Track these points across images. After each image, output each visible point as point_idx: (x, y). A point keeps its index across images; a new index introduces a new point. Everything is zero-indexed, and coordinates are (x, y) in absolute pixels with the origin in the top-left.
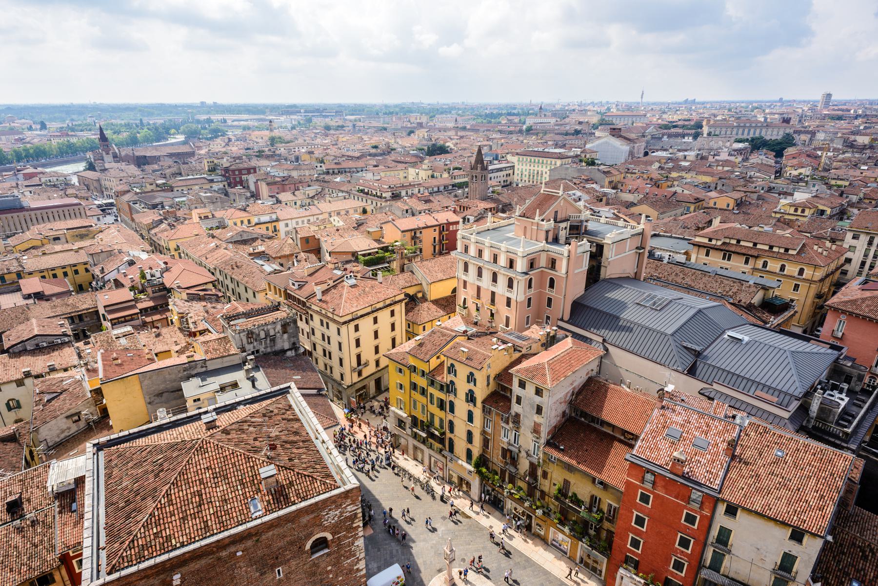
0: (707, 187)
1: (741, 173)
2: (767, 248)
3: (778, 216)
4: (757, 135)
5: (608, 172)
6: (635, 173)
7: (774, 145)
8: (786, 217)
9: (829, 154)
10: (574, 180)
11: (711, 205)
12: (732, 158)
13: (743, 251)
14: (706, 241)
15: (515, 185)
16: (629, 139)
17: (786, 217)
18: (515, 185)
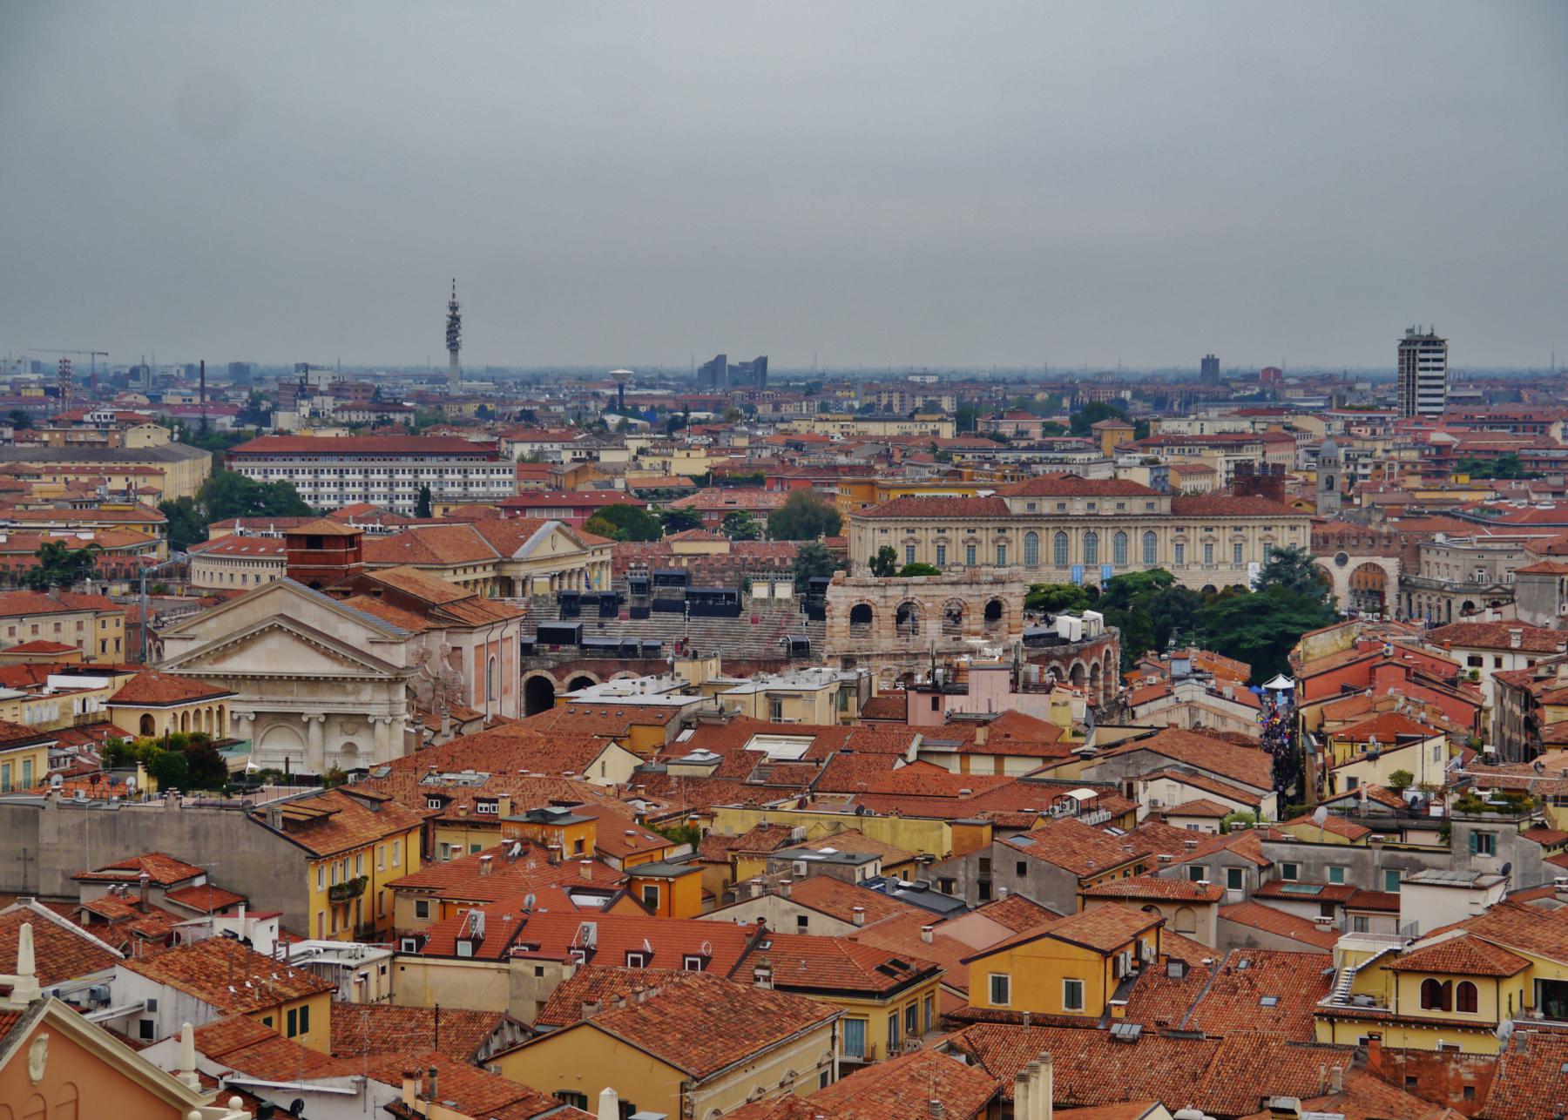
0: (936, 890)
3: (1350, 1035)
4: (1136, 565)
5: (320, 822)
6: (493, 824)
7: (1232, 621)
8: (1394, 1039)
9: (1508, 663)
10: (90, 897)
11: (981, 998)
12: (1032, 705)
16: (417, 606)
17: (1394, 1039)
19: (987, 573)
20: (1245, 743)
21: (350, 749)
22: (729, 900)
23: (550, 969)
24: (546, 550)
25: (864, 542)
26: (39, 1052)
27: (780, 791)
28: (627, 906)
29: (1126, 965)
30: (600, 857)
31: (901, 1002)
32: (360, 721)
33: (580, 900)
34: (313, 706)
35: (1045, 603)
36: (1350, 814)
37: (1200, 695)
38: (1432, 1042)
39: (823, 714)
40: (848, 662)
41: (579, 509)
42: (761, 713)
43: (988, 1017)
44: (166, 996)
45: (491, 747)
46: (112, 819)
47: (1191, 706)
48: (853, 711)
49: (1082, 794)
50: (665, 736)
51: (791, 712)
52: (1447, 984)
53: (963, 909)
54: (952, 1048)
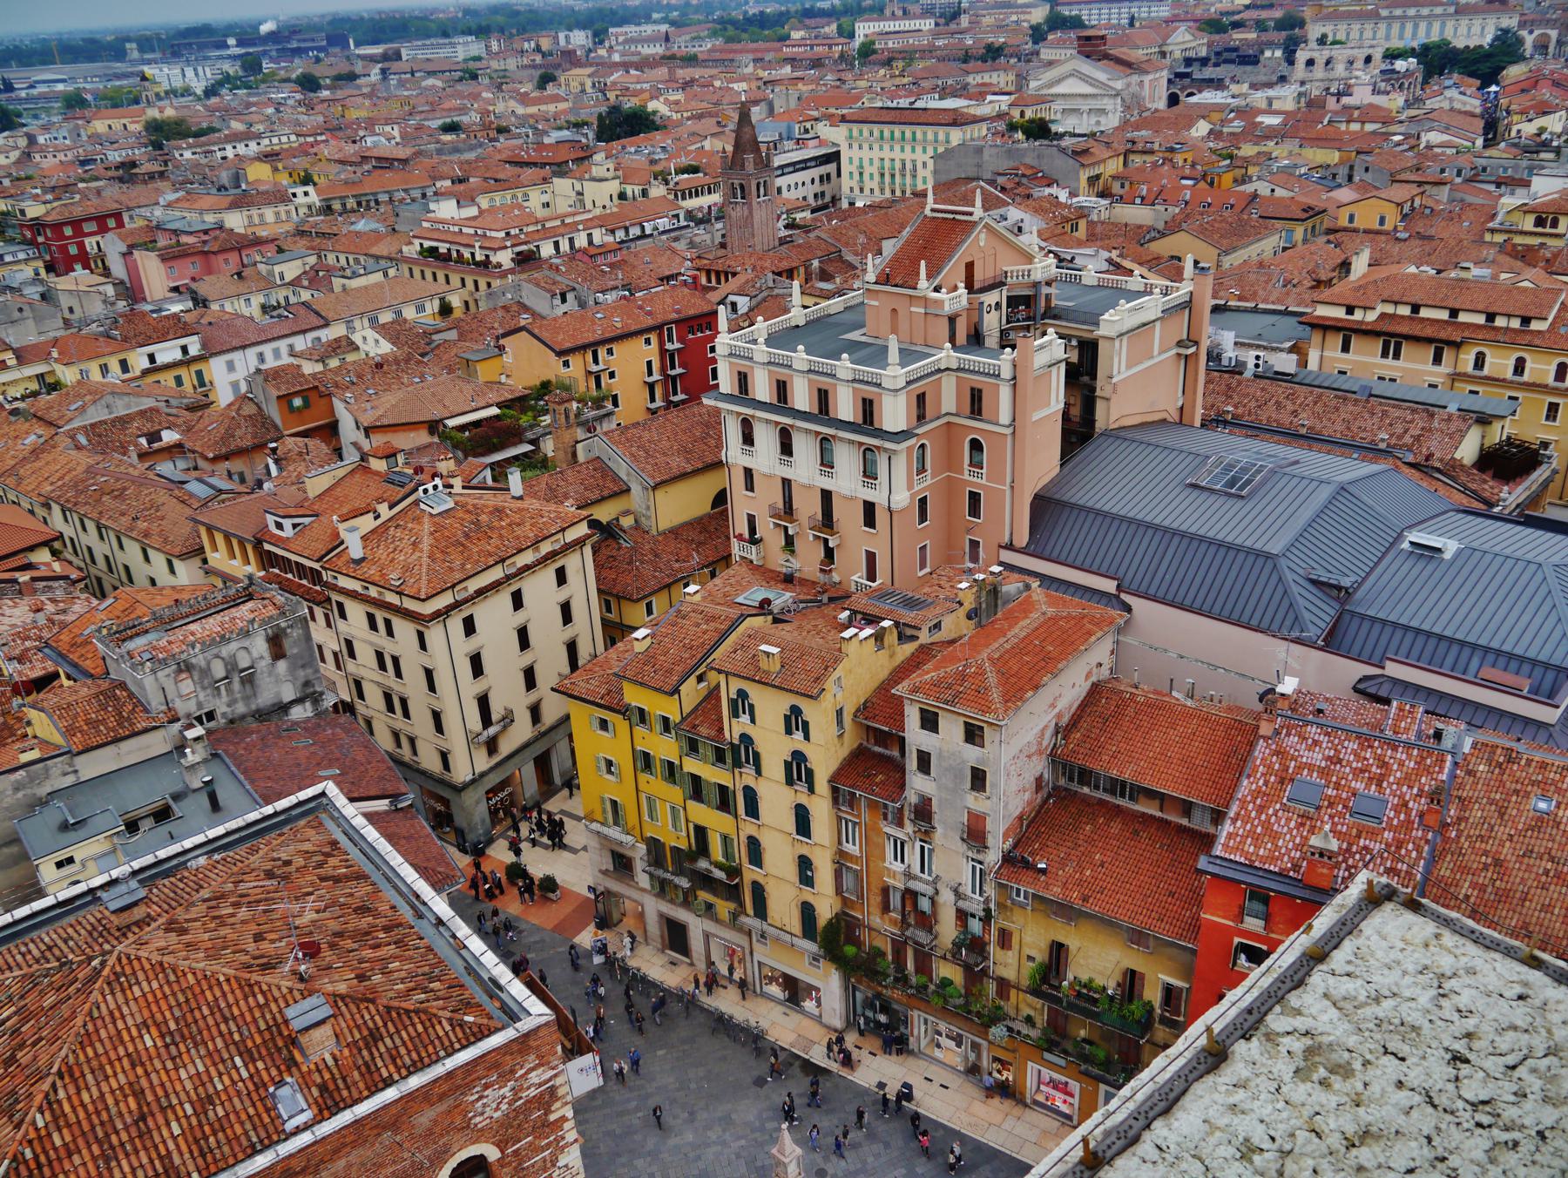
0: (1330, 178)
1: (1407, 136)
2: (1480, 319)
3: (1499, 238)
4: (1435, 37)
5: (1085, 152)
6: (1152, 152)
7: (1476, 61)
8: (1518, 240)
11: (1343, 222)
12: (1380, 100)
13: (1429, 332)
14: (1340, 313)
15: (845, 205)
17: (1518, 240)
18: (845, 205)
19: (1368, 43)
20: (1473, 115)
21: (1098, 123)
22: (1243, 182)
23: (1170, 209)
24: (1180, 39)
25: (1314, 31)
26: (983, 236)
27: (1268, 138)
28: (1202, 185)
29: (1406, 209)
30: (1193, 165)
31: (1309, 223)
32: (1102, 111)
33: (1184, 182)
34: (1085, 105)
35: (1391, 56)
36: (1515, 145)
37: (1458, 96)
38: (1536, 241)
39: (1290, 106)
40: (1303, 83)
41: (1196, 21)
42: (1264, 105)
43: (1345, 230)
44: (1027, 217)
45: (1153, 121)
46: (1009, 151)
47: (1451, 100)
48: (1303, 104)
49: (1397, 138)
50: (1223, 116)
51: (1276, 105)
52: (1545, 218)
53: (1340, 186)
54: (1329, 242)
